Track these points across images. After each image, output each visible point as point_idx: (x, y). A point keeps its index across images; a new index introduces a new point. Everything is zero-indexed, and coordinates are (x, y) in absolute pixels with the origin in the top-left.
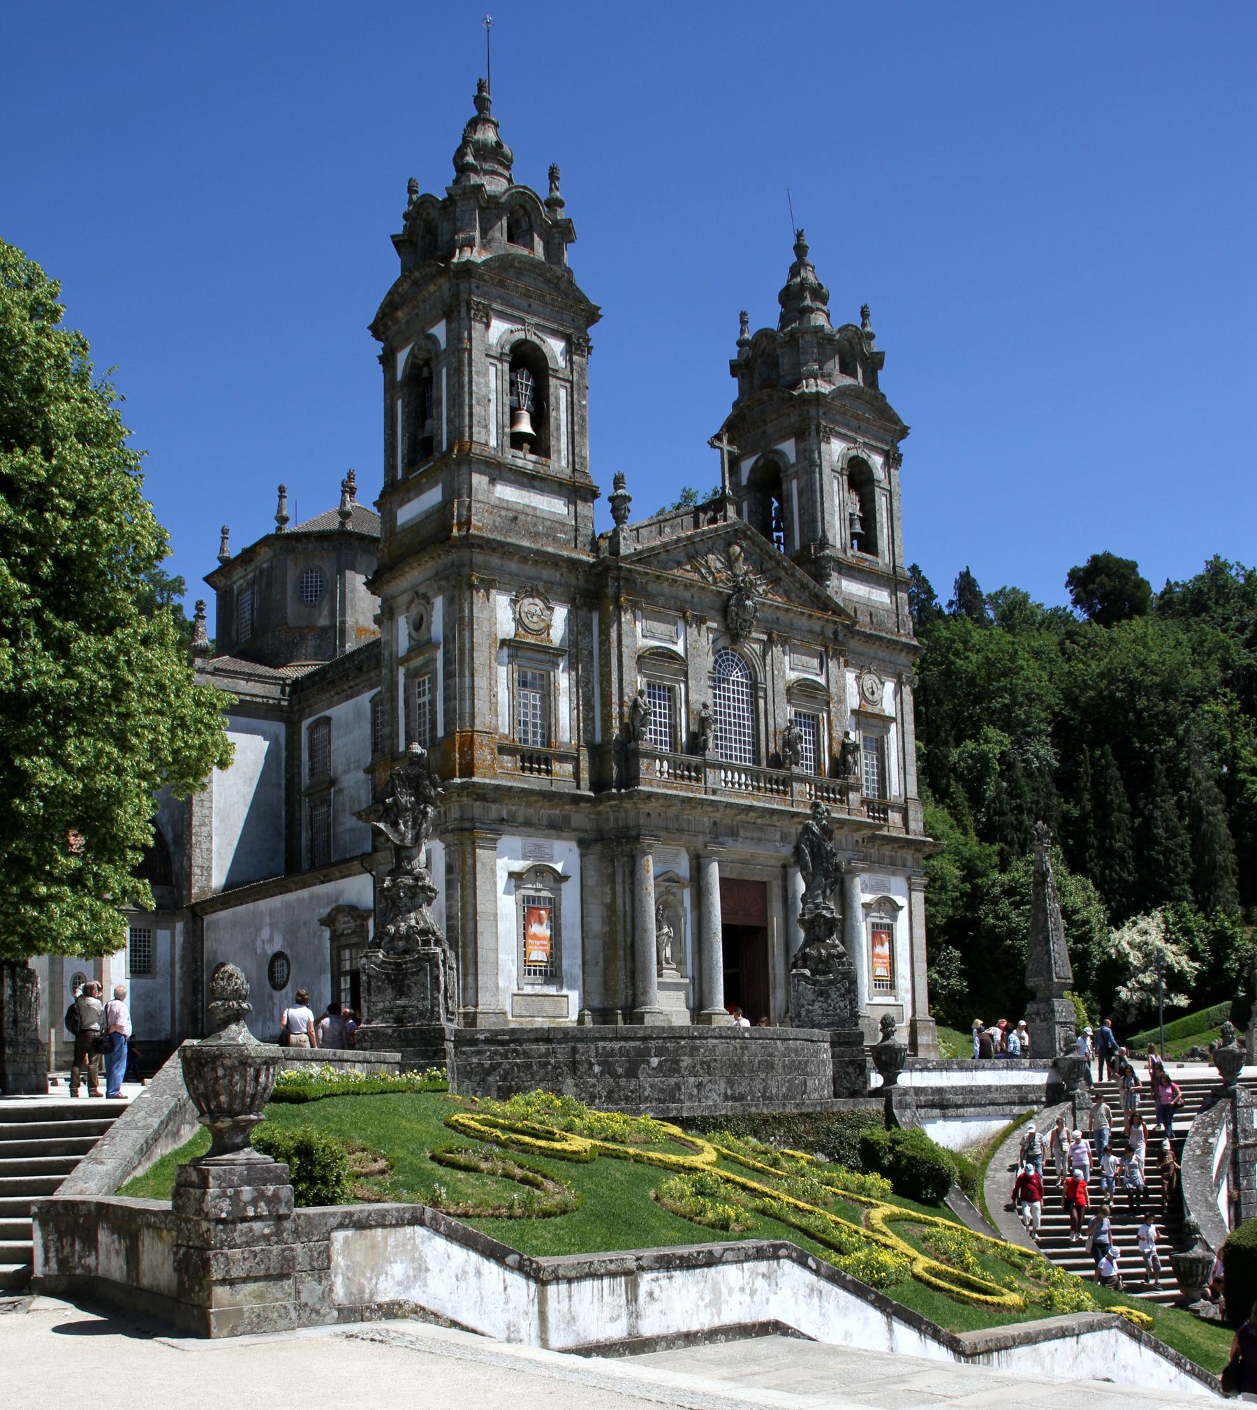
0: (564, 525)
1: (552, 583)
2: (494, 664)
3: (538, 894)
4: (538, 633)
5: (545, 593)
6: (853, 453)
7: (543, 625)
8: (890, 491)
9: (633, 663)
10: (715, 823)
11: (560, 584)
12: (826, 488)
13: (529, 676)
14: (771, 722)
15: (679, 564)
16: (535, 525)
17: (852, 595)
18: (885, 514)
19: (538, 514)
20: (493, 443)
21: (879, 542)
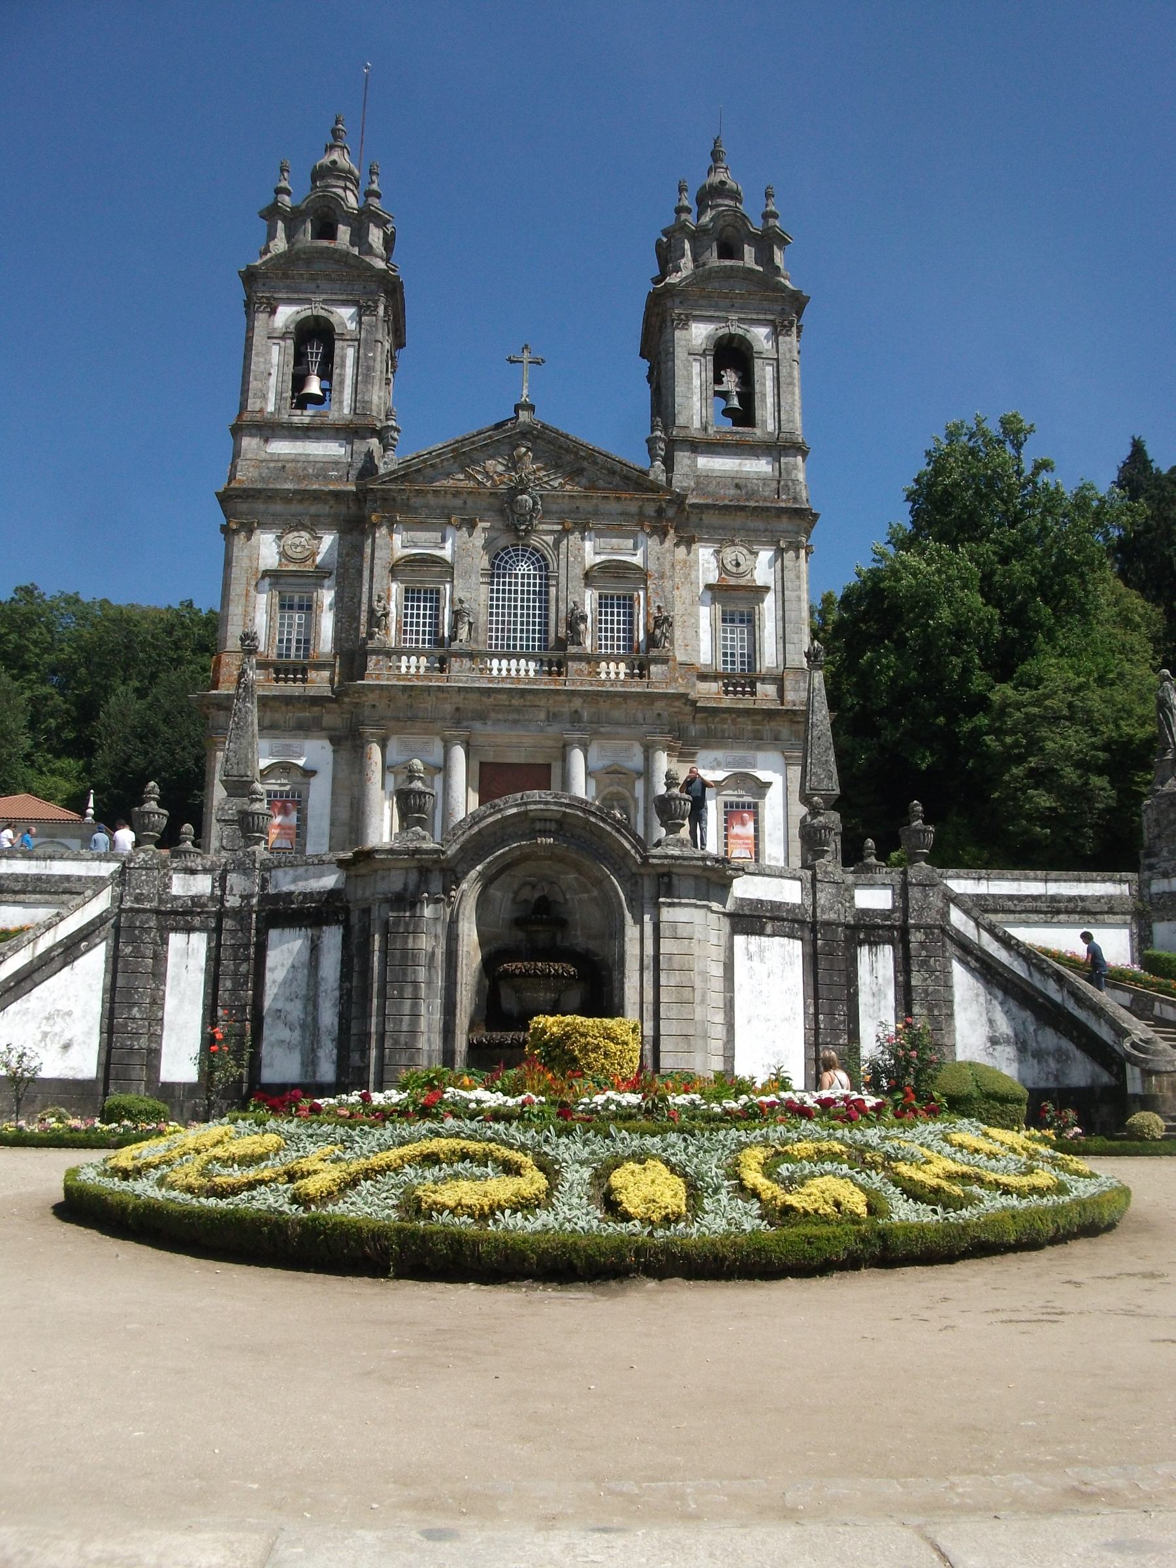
0: (337, 463)
1: (319, 516)
2: (253, 592)
3: (282, 788)
4: (304, 560)
5: (313, 526)
6: (721, 332)
7: (307, 553)
8: (777, 360)
9: (386, 573)
10: (458, 709)
11: (329, 515)
12: (679, 371)
13: (296, 599)
14: (562, 607)
15: (448, 475)
16: (305, 469)
17: (713, 471)
18: (769, 384)
19: (311, 458)
20: (271, 408)
21: (758, 414)
